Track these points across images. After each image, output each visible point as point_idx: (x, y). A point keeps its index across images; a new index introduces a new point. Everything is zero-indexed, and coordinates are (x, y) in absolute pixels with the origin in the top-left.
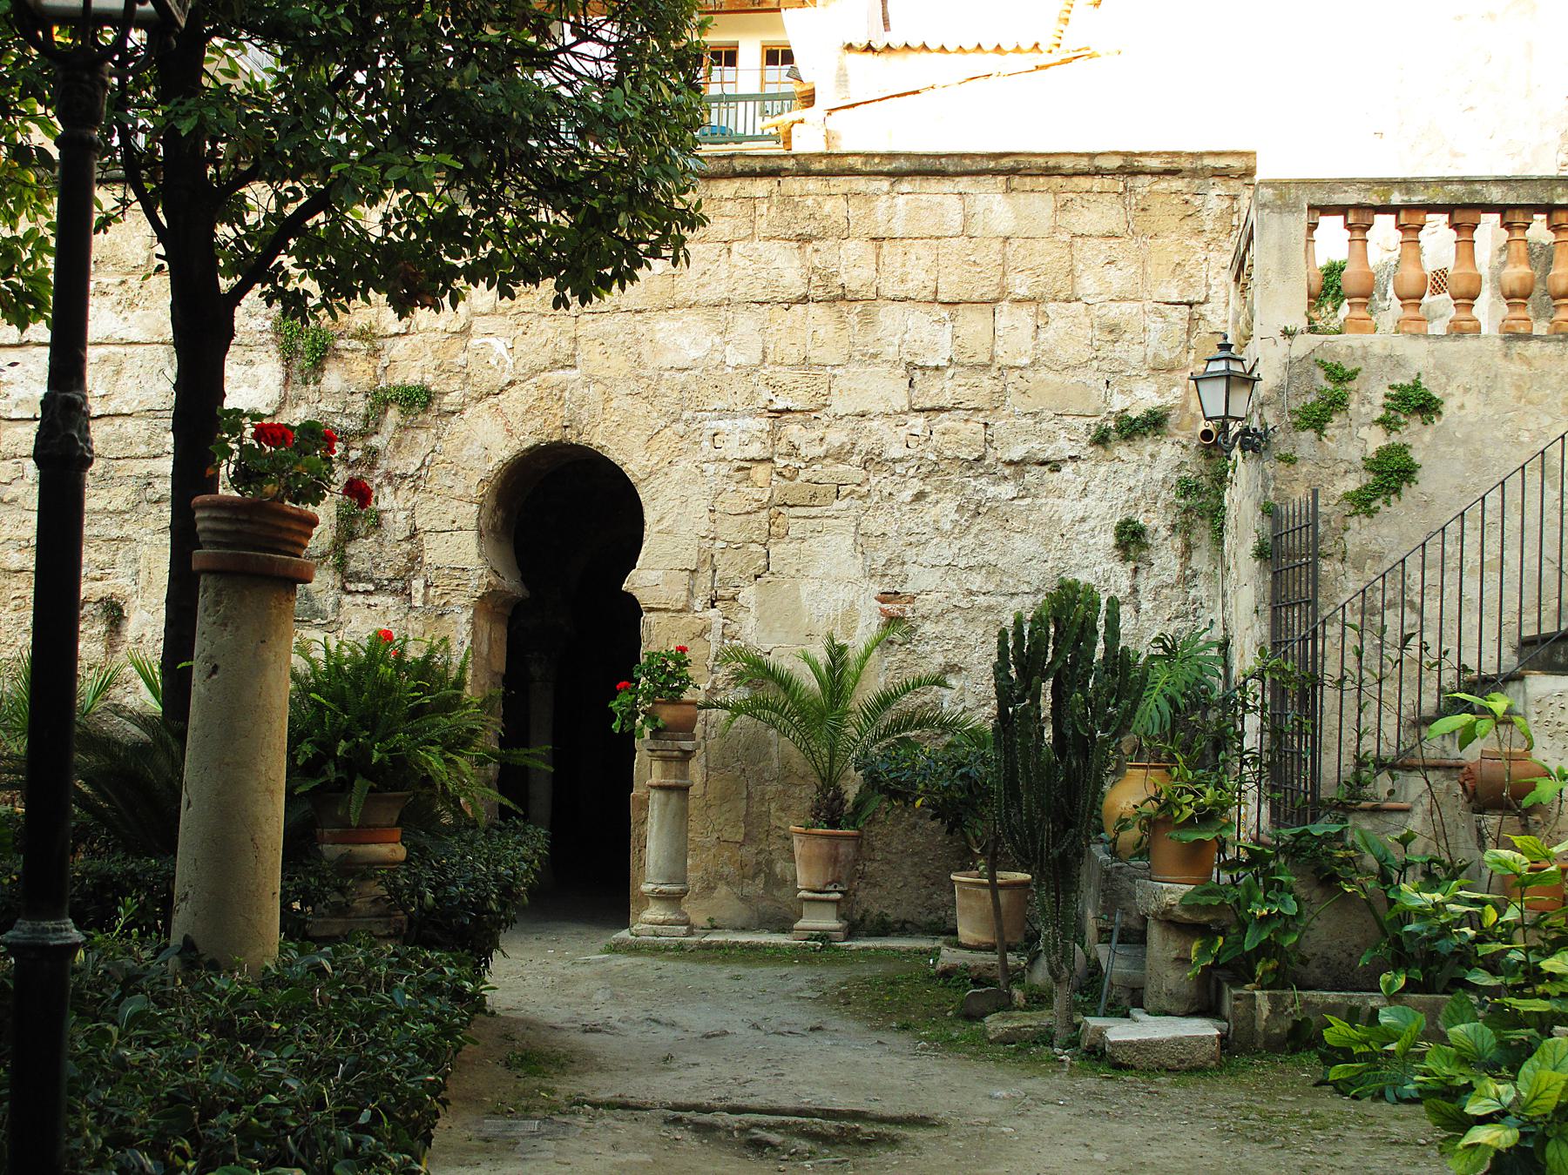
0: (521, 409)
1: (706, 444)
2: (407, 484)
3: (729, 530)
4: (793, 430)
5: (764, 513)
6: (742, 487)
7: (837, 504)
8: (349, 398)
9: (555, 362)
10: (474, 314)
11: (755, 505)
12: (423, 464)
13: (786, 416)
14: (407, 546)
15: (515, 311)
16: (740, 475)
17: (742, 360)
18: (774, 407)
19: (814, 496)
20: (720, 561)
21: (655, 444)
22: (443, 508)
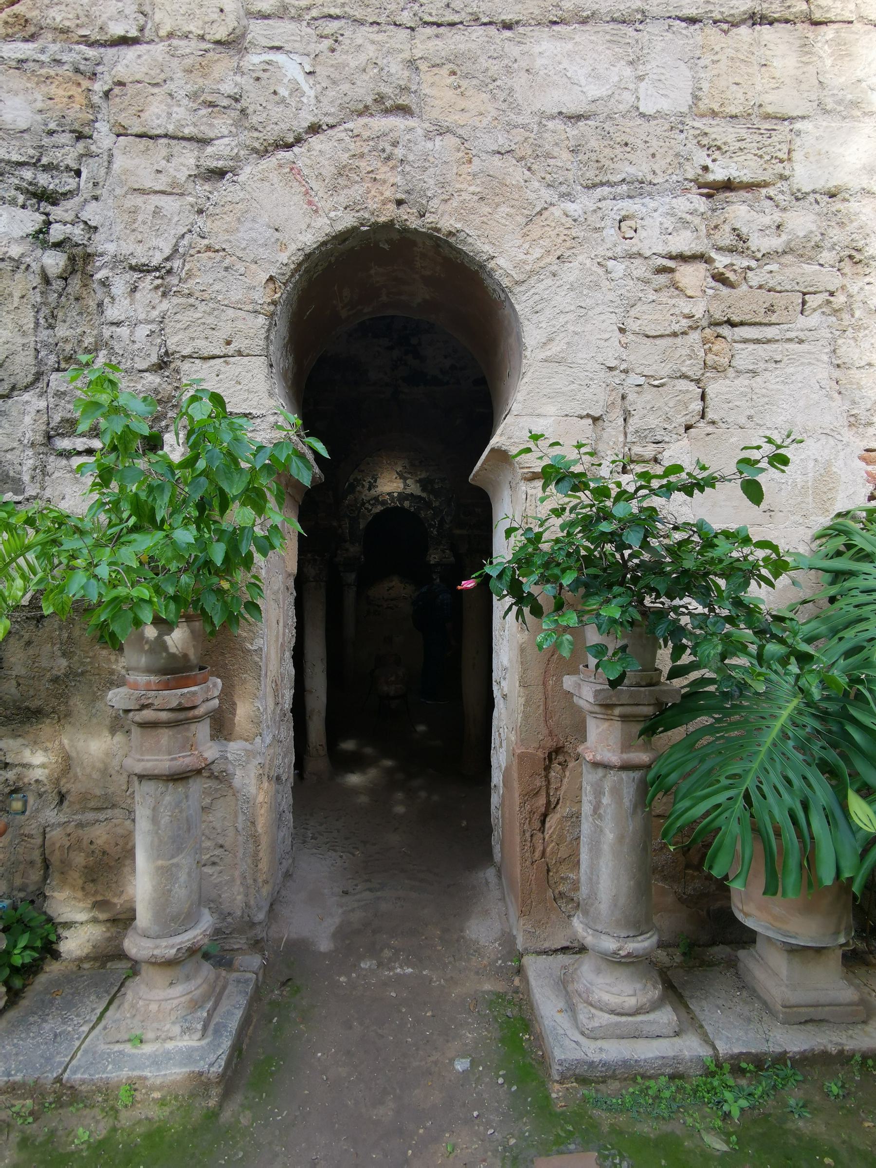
0: (329, 170)
1: (611, 232)
2: (147, 282)
3: (648, 358)
4: (739, 212)
5: (695, 336)
6: (663, 297)
7: (802, 321)
8: (46, 141)
9: (380, 99)
10: (249, 14)
11: (685, 323)
12: (176, 251)
13: (722, 196)
14: (153, 380)
15: (314, 13)
16: (663, 279)
17: (665, 105)
18: (710, 177)
19: (771, 310)
20: (638, 402)
21: (535, 230)
22: (210, 320)
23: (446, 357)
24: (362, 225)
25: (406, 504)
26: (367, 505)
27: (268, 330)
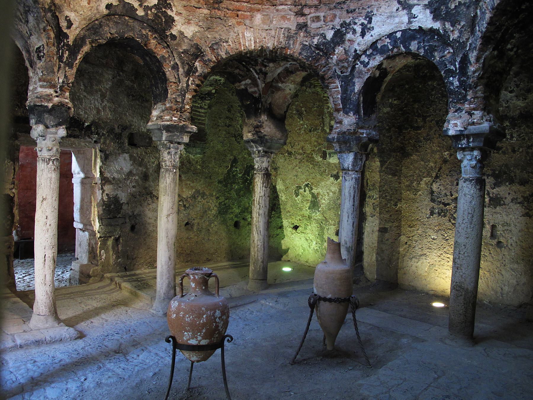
25: (414, 46)
26: (364, 58)
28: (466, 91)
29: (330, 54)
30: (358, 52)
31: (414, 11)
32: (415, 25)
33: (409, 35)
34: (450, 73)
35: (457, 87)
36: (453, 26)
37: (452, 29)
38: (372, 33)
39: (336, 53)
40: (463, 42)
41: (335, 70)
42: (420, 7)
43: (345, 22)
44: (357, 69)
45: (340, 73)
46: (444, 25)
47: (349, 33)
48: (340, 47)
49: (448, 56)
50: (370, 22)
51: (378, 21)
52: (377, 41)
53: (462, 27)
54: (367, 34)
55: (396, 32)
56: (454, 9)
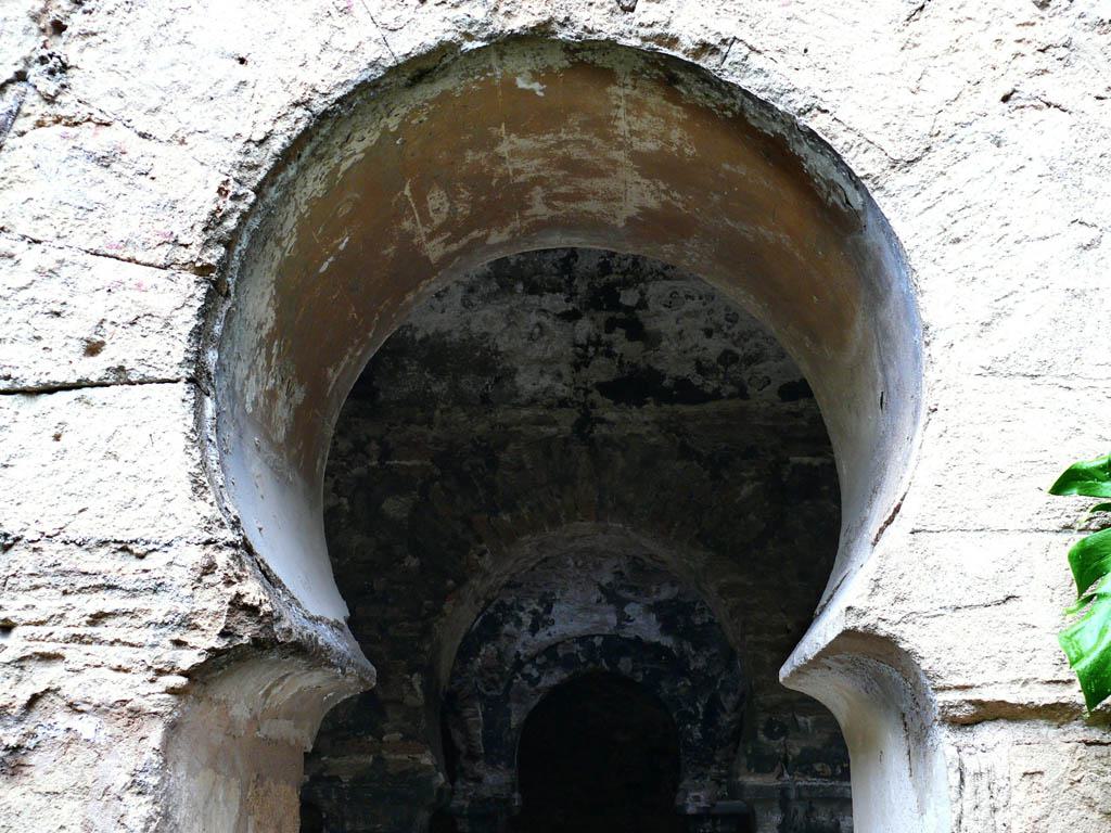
22: (50, 291)
23: (709, 333)
24: (469, 37)
25: (625, 664)
26: (528, 668)
27: (203, 313)
28: (715, 749)
29: (472, 656)
30: (521, 658)
31: (628, 610)
32: (629, 632)
33: (617, 645)
34: (692, 718)
35: (699, 740)
36: (695, 648)
37: (693, 652)
38: (551, 629)
39: (481, 653)
40: (713, 676)
41: (476, 684)
42: (638, 607)
43: (502, 602)
44: (515, 686)
45: (483, 690)
46: (682, 645)
47: (508, 622)
48: (489, 645)
49: (683, 690)
50: (548, 610)
51: (561, 612)
52: (558, 644)
53: (715, 655)
54: (541, 629)
55: (594, 636)
56: (700, 626)
